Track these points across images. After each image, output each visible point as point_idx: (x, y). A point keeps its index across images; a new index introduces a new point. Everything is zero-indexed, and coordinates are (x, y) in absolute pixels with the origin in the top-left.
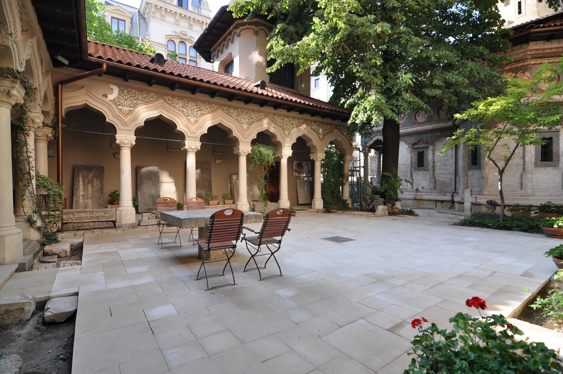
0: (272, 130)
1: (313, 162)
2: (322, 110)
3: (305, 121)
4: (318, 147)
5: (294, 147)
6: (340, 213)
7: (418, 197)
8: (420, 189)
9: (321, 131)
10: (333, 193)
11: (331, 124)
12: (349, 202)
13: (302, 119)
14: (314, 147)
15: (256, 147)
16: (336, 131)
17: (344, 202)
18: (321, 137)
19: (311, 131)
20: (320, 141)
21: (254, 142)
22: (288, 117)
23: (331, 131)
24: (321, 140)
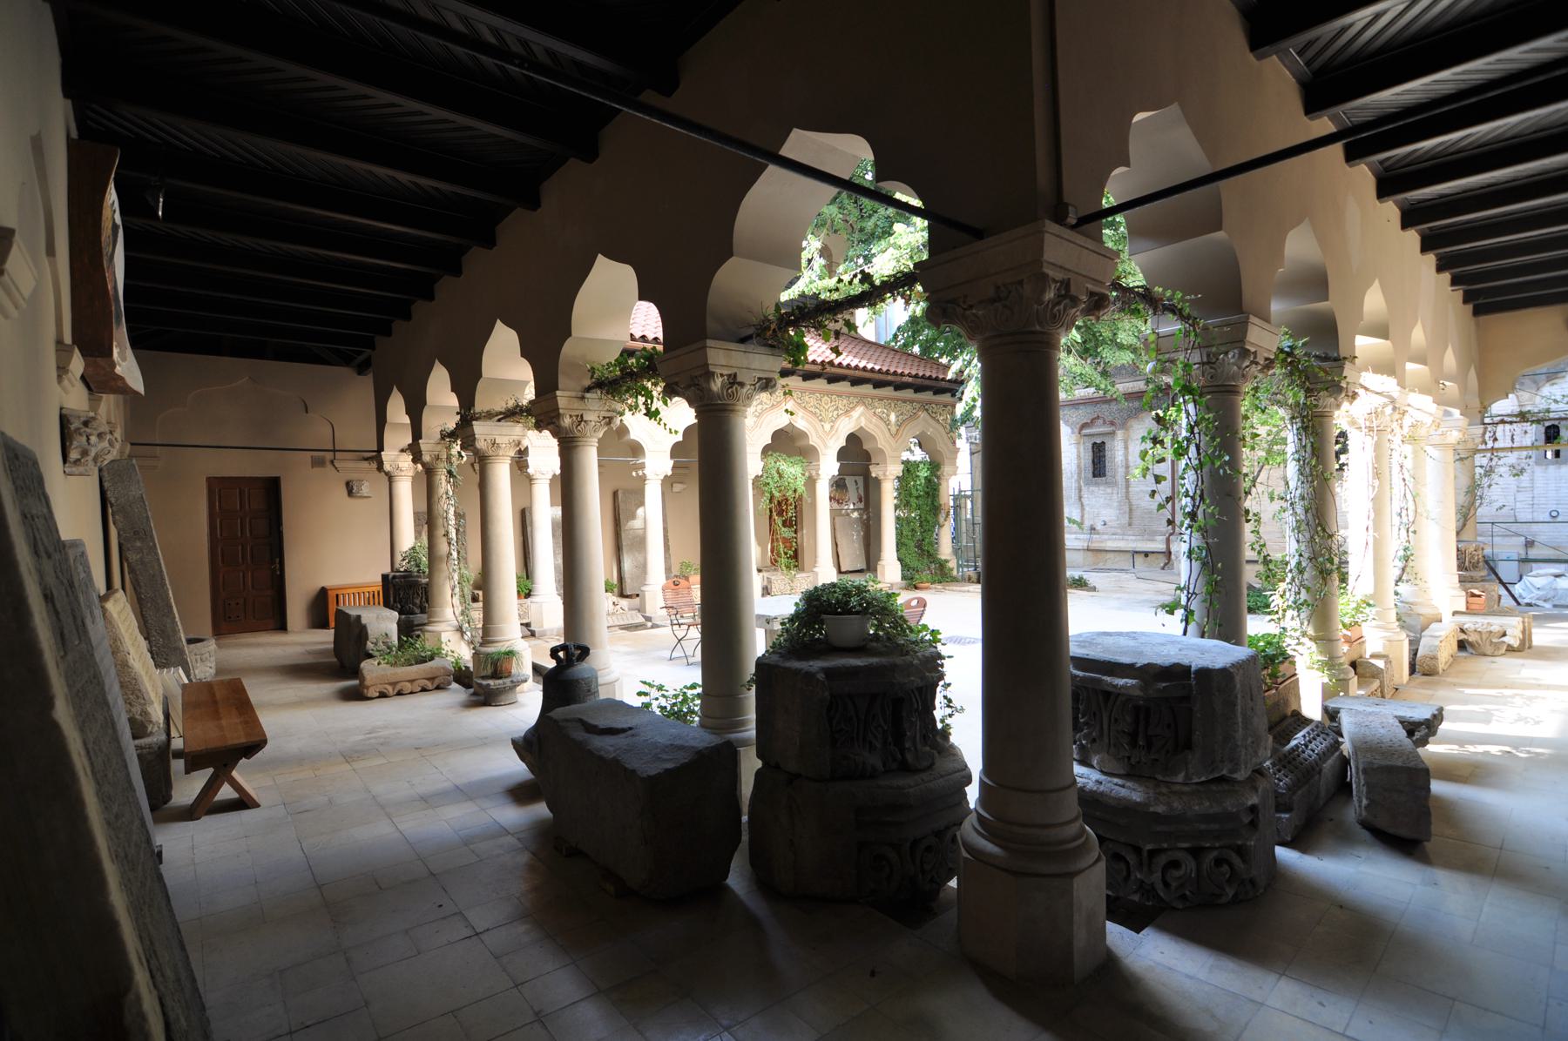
0: (801, 423)
1: (878, 482)
2: (898, 379)
3: (862, 400)
4: (888, 451)
5: (842, 454)
6: (938, 591)
7: (1095, 545)
8: (1099, 527)
9: (893, 417)
10: (919, 547)
11: (912, 401)
12: (952, 564)
13: (855, 396)
14: (881, 451)
15: (771, 460)
16: (923, 415)
17: (942, 565)
18: (894, 429)
19: (874, 420)
20: (891, 440)
21: (766, 451)
22: (829, 394)
23: (913, 416)
24: (893, 436)
